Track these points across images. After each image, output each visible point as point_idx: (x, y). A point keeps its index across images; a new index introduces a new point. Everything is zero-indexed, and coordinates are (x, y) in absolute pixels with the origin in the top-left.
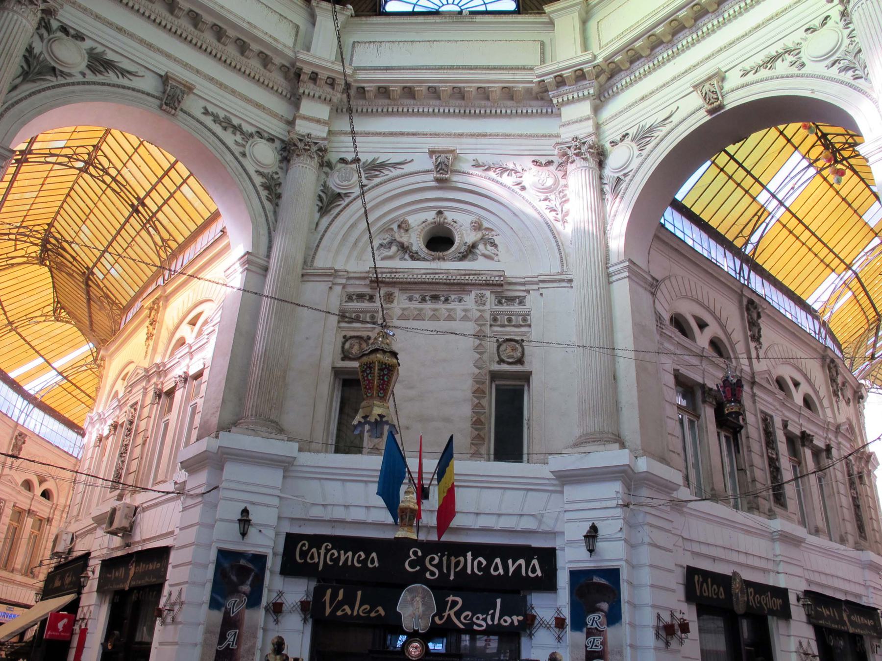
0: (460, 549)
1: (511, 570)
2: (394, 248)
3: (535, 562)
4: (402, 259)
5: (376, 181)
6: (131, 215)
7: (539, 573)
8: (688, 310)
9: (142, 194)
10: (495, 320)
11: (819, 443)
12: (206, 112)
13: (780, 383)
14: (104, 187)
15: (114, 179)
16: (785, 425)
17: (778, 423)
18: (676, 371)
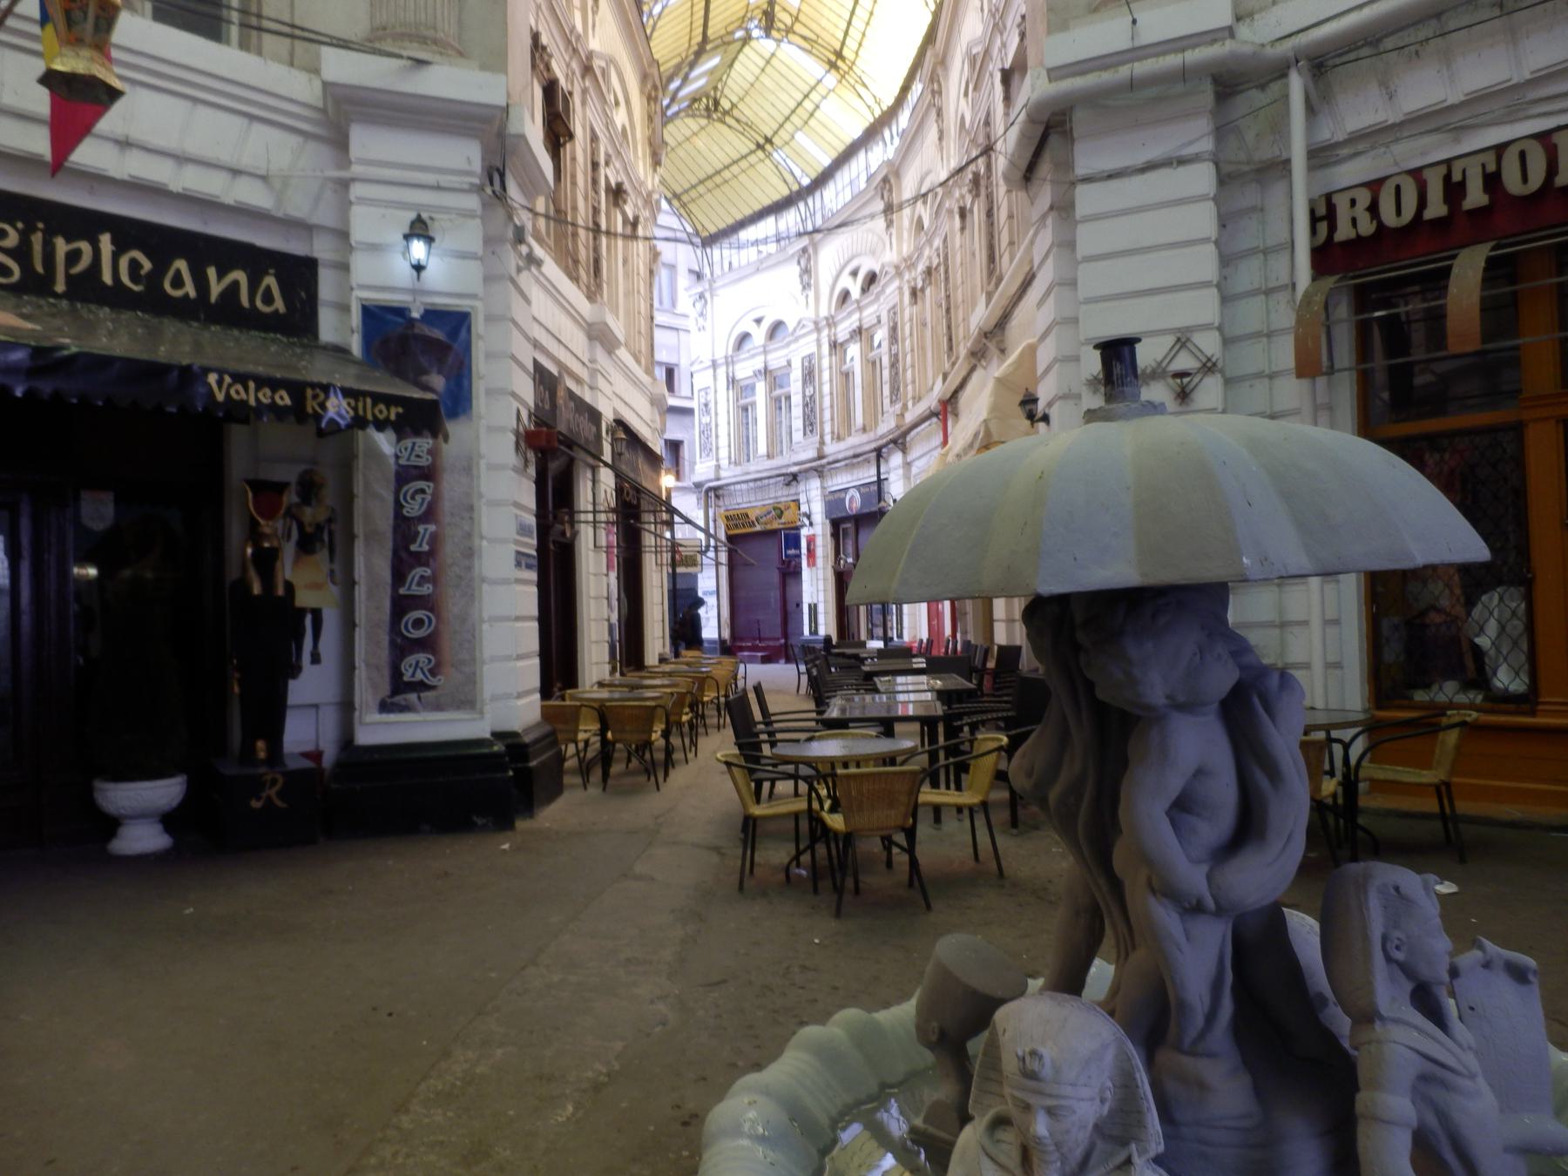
0: (85, 224)
1: (216, 289)
3: (270, 281)
7: (279, 305)
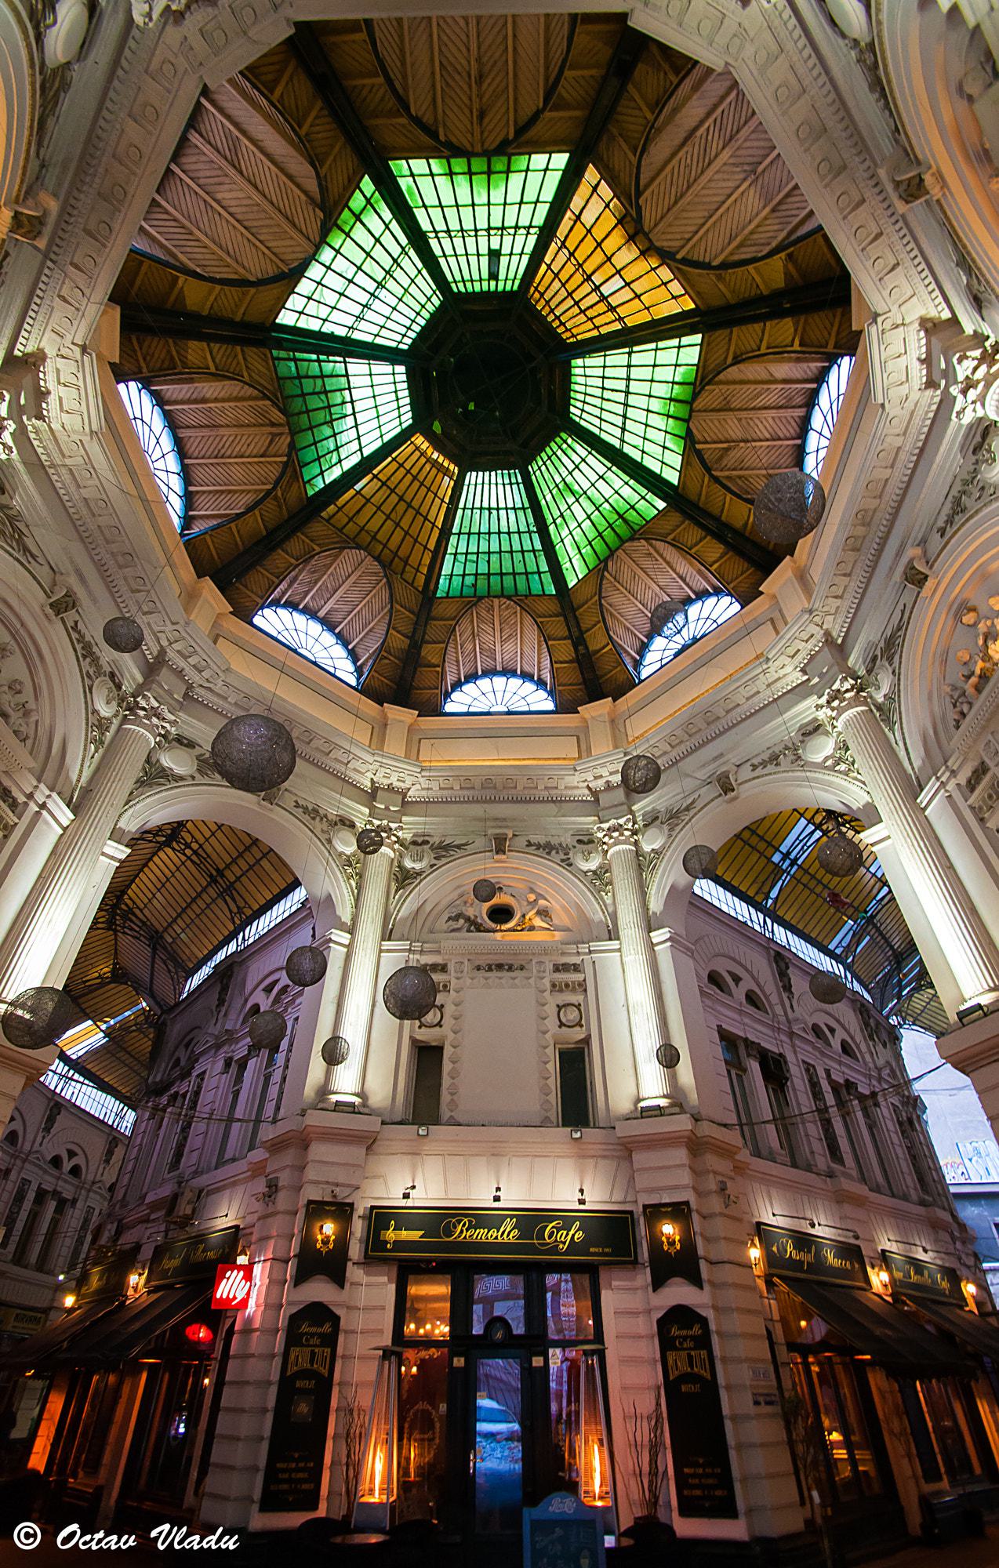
2: (462, 921)
4: (469, 931)
5: (444, 860)
6: (209, 884)
8: (722, 967)
9: (222, 866)
10: (554, 986)
11: (864, 1089)
12: (297, 806)
13: (816, 1029)
14: (184, 858)
15: (195, 852)
16: (828, 1072)
17: (821, 1074)
18: (719, 1027)
